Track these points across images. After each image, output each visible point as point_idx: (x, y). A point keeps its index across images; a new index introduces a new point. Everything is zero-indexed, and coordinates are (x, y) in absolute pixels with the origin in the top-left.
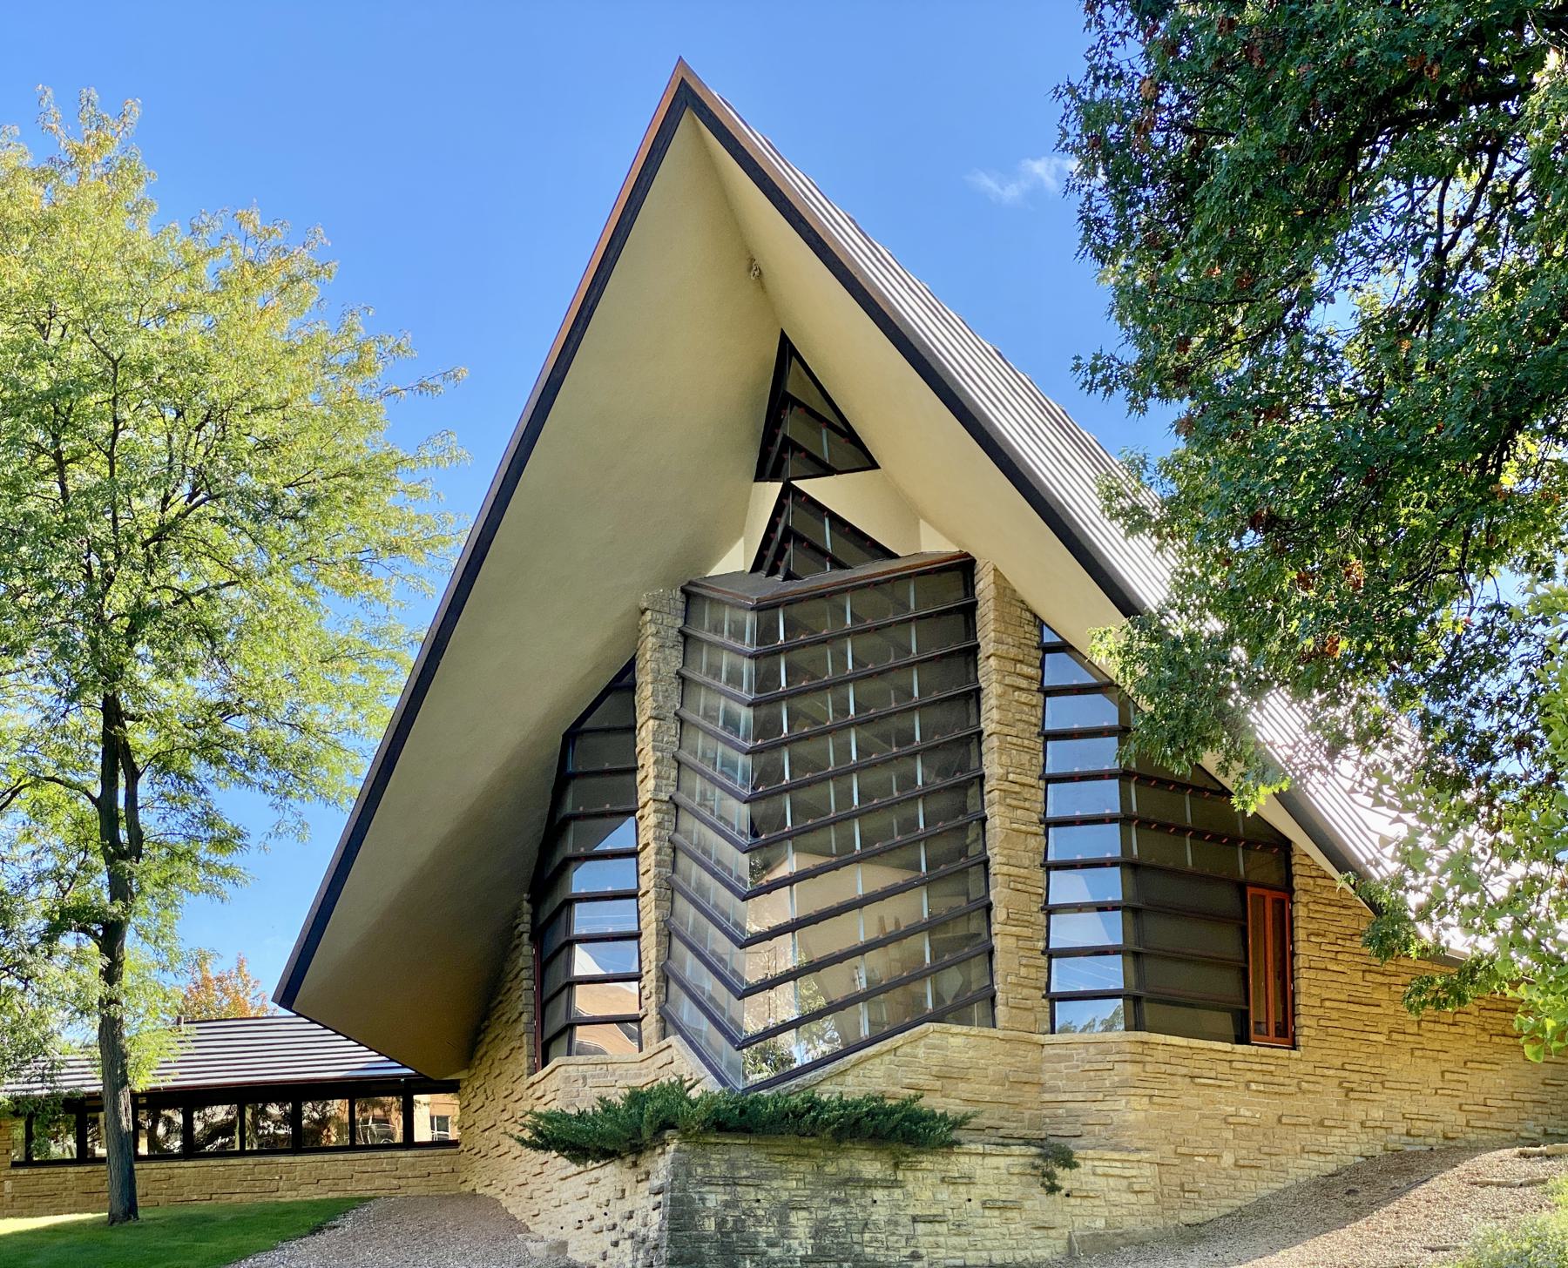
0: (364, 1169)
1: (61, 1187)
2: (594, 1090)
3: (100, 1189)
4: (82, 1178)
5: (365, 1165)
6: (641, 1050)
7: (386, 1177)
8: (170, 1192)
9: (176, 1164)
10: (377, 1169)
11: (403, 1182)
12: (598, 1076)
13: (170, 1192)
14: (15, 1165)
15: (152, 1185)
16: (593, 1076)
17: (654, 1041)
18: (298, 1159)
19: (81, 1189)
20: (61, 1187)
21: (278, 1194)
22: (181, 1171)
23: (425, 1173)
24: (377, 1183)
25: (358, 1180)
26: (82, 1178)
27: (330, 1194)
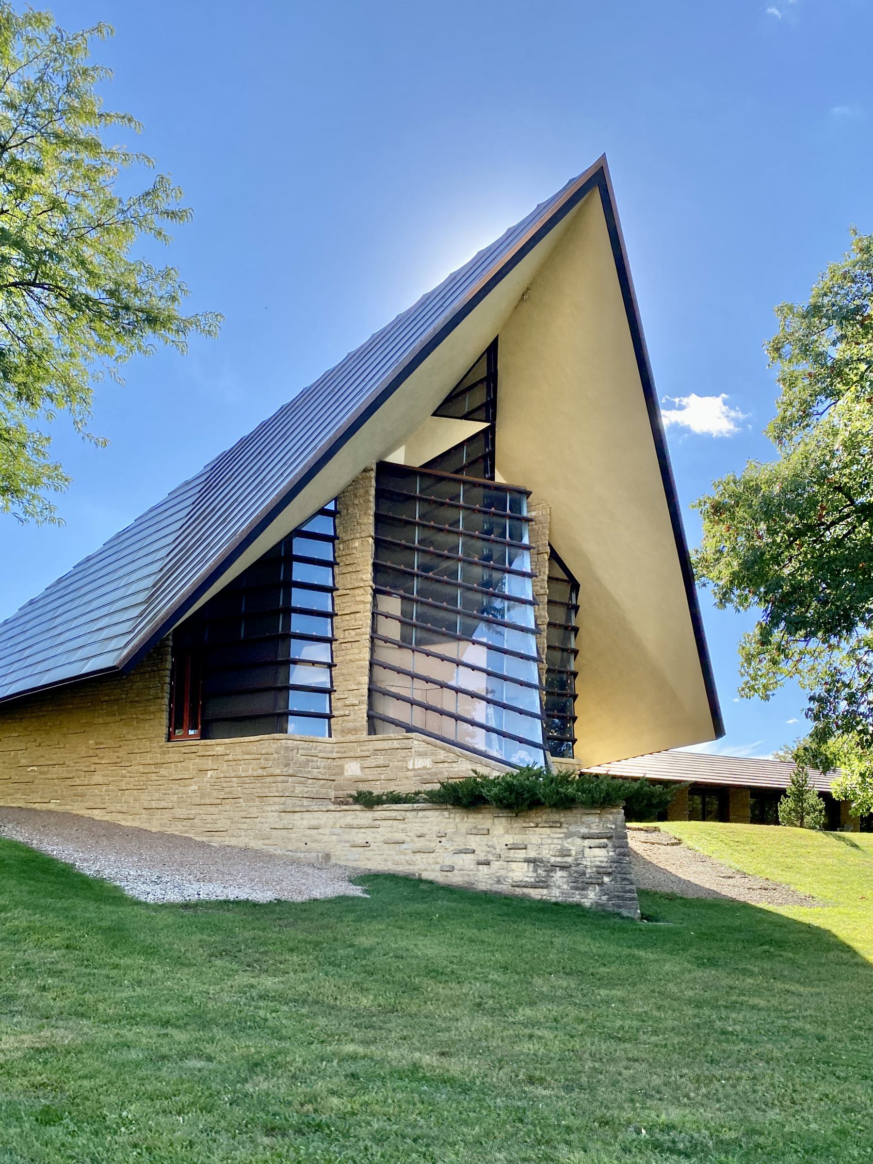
2: (304, 757)
6: (330, 736)
12: (307, 749)
16: (303, 749)
17: (365, 733)
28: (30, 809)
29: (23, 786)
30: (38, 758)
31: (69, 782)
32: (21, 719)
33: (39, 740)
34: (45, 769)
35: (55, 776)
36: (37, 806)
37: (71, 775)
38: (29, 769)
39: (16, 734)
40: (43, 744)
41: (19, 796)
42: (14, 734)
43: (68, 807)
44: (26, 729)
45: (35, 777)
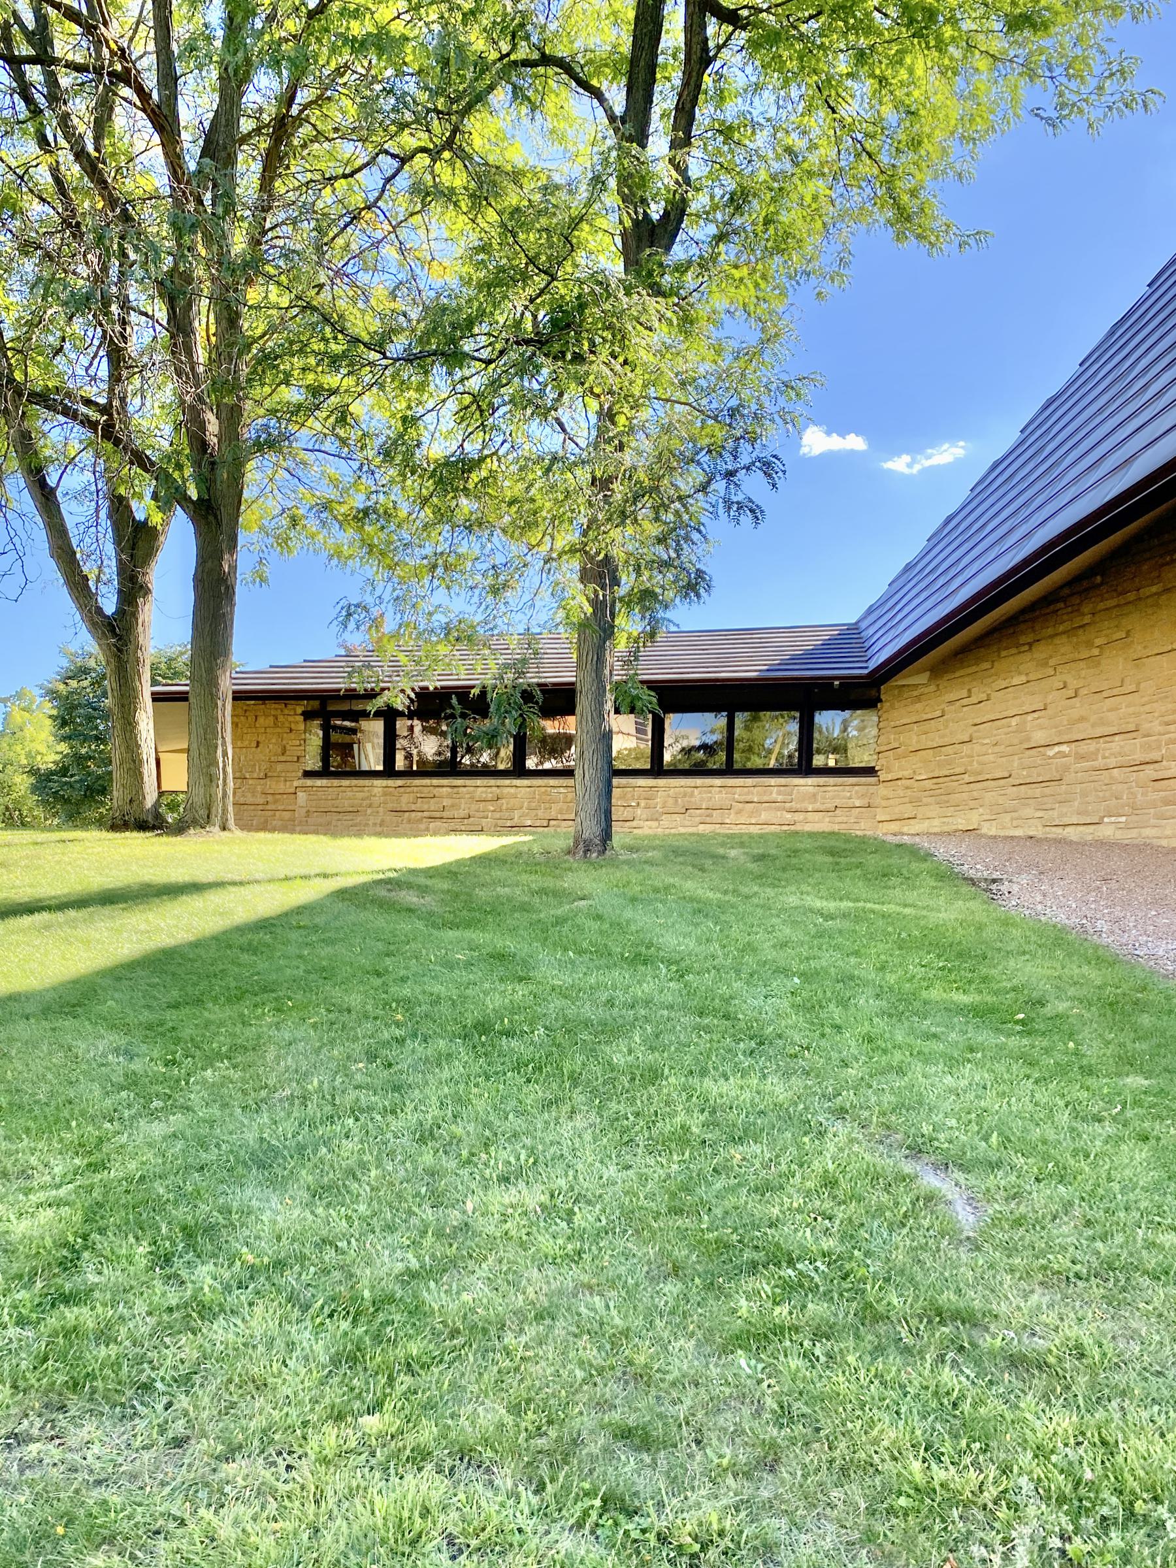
0: (748, 798)
1: (365, 803)
3: (413, 807)
4: (391, 794)
5: (748, 793)
7: (778, 809)
8: (497, 815)
9: (507, 782)
10: (766, 798)
11: (799, 817)
13: (497, 815)
14: (308, 774)
15: (474, 807)
18: (661, 782)
19: (390, 806)
20: (365, 803)
21: (634, 824)
22: (512, 790)
23: (831, 806)
24: (764, 817)
25: (739, 812)
26: (391, 794)
27: (702, 827)
28: (1059, 842)
29: (1037, 791)
30: (1072, 722)
31: (1150, 772)
32: (1030, 645)
33: (1073, 683)
34: (1092, 746)
35: (1112, 762)
36: (1072, 833)
37: (1155, 756)
38: (1051, 752)
39: (1023, 679)
40: (1083, 692)
41: (1028, 812)
42: (1016, 681)
43: (1147, 832)
44: (1044, 664)
45: (1067, 769)
